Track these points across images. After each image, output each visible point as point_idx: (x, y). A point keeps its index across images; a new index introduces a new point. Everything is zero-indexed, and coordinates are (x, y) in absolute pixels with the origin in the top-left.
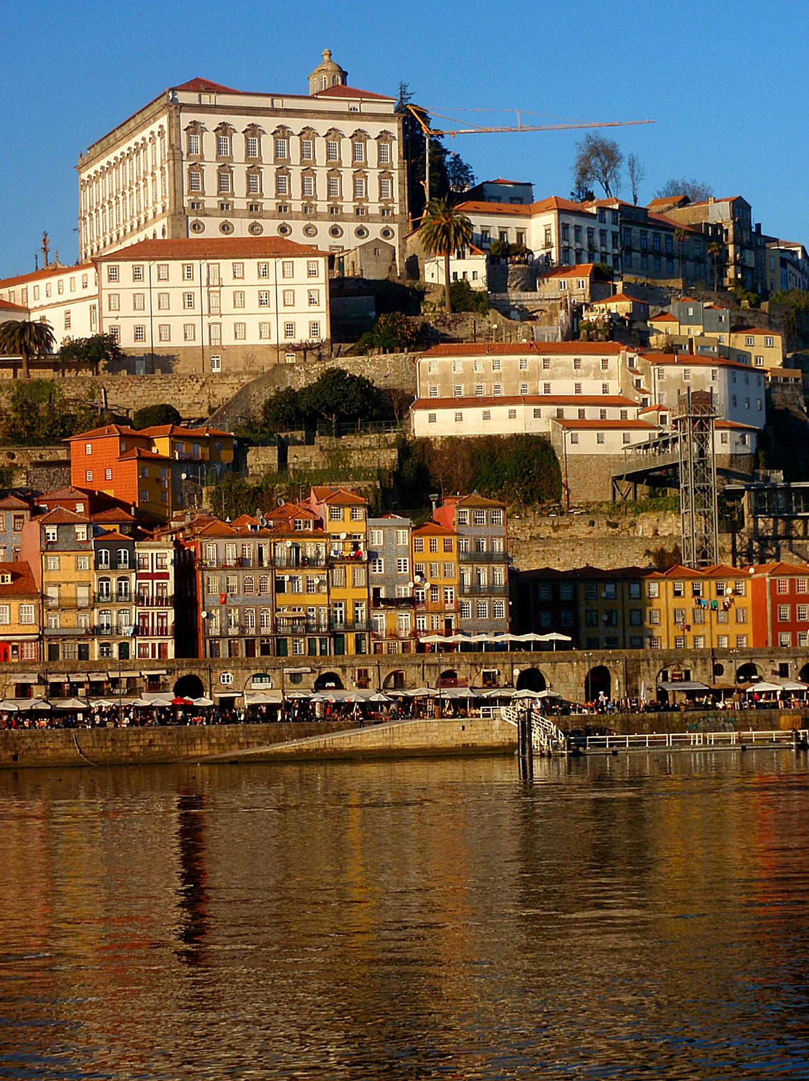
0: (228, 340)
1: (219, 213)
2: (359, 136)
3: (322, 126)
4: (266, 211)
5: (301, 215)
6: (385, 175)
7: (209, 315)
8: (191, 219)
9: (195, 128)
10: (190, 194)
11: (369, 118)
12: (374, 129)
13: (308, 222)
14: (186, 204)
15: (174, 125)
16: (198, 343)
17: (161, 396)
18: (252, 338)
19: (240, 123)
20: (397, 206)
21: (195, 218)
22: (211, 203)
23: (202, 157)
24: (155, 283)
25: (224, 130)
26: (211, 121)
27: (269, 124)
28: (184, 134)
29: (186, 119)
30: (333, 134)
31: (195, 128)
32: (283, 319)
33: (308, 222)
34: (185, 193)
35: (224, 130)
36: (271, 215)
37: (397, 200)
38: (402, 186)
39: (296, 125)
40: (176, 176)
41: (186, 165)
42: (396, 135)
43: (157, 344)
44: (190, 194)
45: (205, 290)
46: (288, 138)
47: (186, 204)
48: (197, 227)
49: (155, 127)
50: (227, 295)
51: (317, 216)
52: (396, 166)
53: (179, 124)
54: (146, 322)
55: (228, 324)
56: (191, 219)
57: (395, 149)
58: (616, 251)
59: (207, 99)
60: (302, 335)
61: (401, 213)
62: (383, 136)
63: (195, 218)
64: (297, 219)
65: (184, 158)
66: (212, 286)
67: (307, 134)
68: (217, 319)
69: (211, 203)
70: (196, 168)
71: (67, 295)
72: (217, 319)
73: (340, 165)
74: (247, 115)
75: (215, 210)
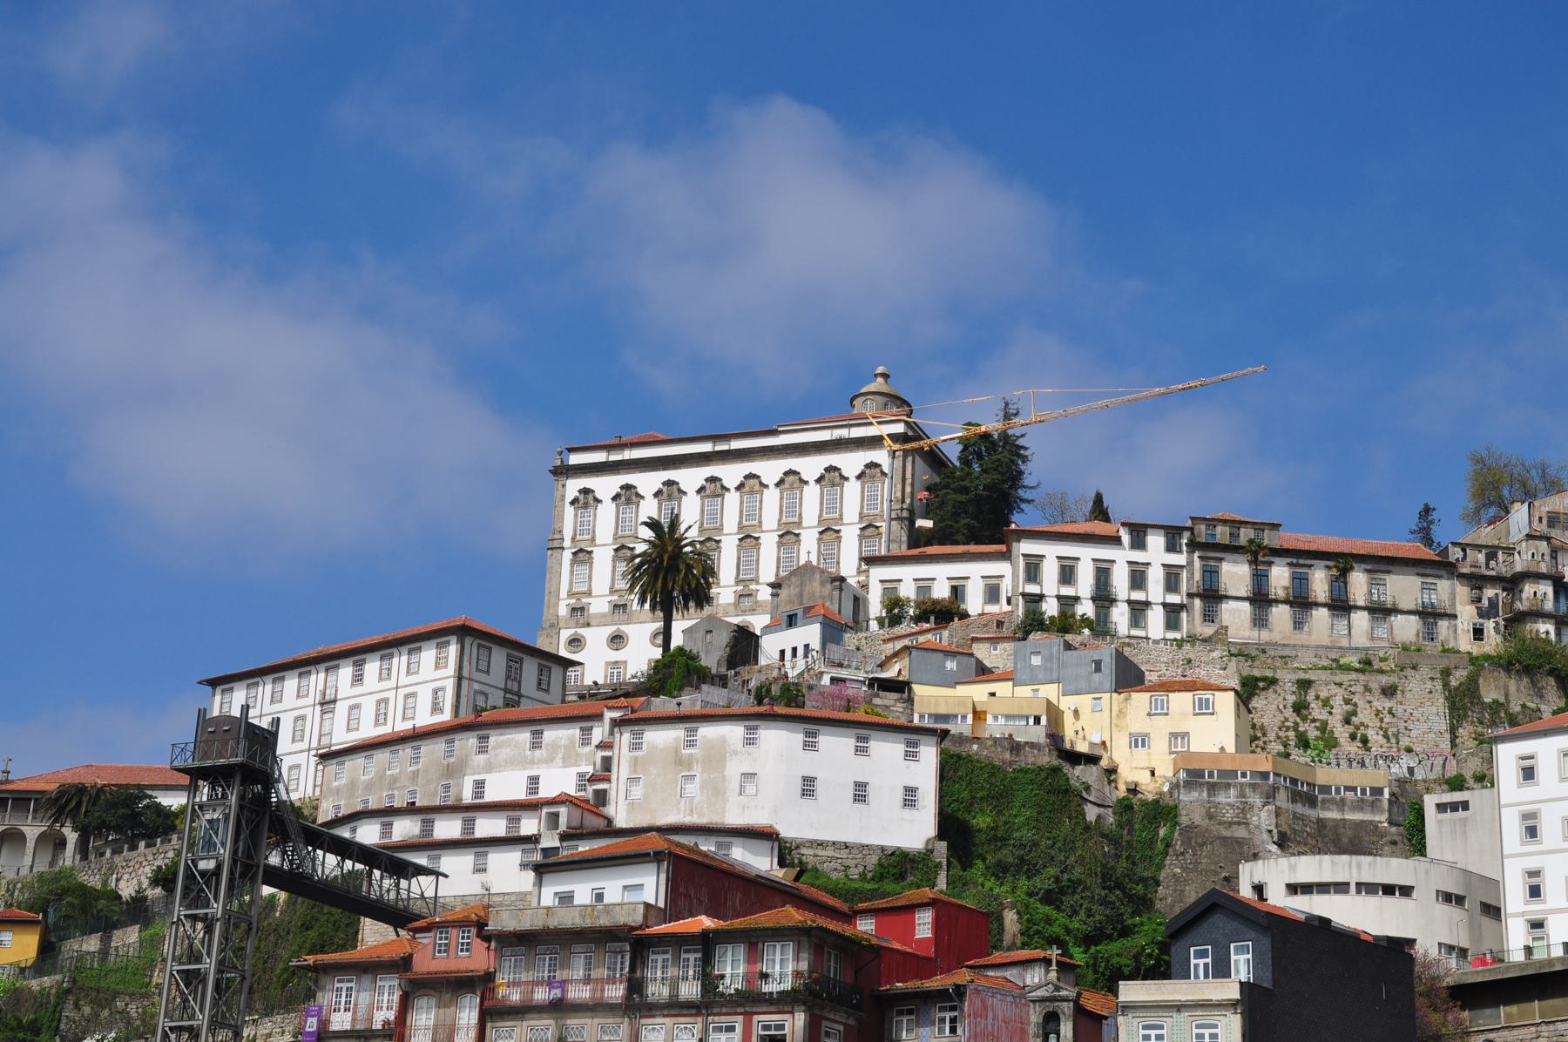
1: (609, 619)
8: (565, 634)
9: (587, 499)
10: (571, 595)
14: (563, 611)
21: (572, 631)
26: (605, 486)
29: (573, 486)
31: (587, 499)
39: (731, 473)
41: (567, 556)
46: (722, 496)
53: (563, 496)
58: (1174, 599)
63: (572, 631)
65: (567, 543)
73: (799, 524)
75: (603, 615)
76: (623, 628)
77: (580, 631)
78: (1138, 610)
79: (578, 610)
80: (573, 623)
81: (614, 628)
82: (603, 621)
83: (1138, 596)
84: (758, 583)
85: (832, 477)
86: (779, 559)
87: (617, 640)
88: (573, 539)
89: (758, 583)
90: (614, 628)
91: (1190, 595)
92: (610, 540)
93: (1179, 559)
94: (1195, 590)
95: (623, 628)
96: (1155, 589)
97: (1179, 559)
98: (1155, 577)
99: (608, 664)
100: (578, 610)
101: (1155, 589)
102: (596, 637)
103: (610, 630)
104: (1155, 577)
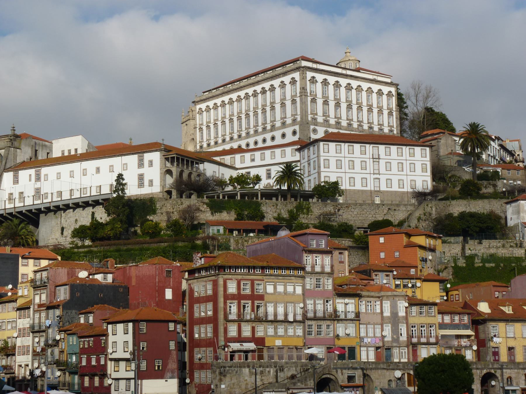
0: (383, 188)
2: (380, 93)
3: (365, 86)
6: (390, 114)
7: (374, 174)
8: (312, 127)
10: (311, 114)
11: (384, 84)
12: (386, 89)
14: (310, 119)
15: (303, 78)
16: (368, 188)
17: (366, 215)
18: (395, 188)
19: (332, 80)
20: (395, 130)
23: (316, 95)
24: (347, 155)
25: (325, 83)
26: (320, 77)
27: (344, 82)
28: (308, 83)
29: (309, 75)
30: (370, 91)
31: (313, 80)
32: (410, 178)
34: (309, 113)
35: (325, 83)
37: (395, 127)
39: (355, 84)
40: (303, 103)
41: (309, 99)
42: (394, 95)
43: (348, 188)
44: (311, 114)
45: (372, 160)
47: (310, 119)
48: (315, 131)
49: (287, 79)
50: (382, 163)
52: (394, 109)
54: (343, 175)
55: (383, 178)
56: (312, 127)
57: (394, 100)
59: (315, 66)
60: (419, 188)
62: (389, 94)
65: (309, 95)
66: (376, 159)
67: (359, 89)
68: (378, 176)
69: (320, 119)
70: (314, 101)
71: (268, 161)
72: (378, 176)
74: (335, 76)
81: (326, 129)
82: (321, 125)
95: (328, 129)
103: (325, 129)
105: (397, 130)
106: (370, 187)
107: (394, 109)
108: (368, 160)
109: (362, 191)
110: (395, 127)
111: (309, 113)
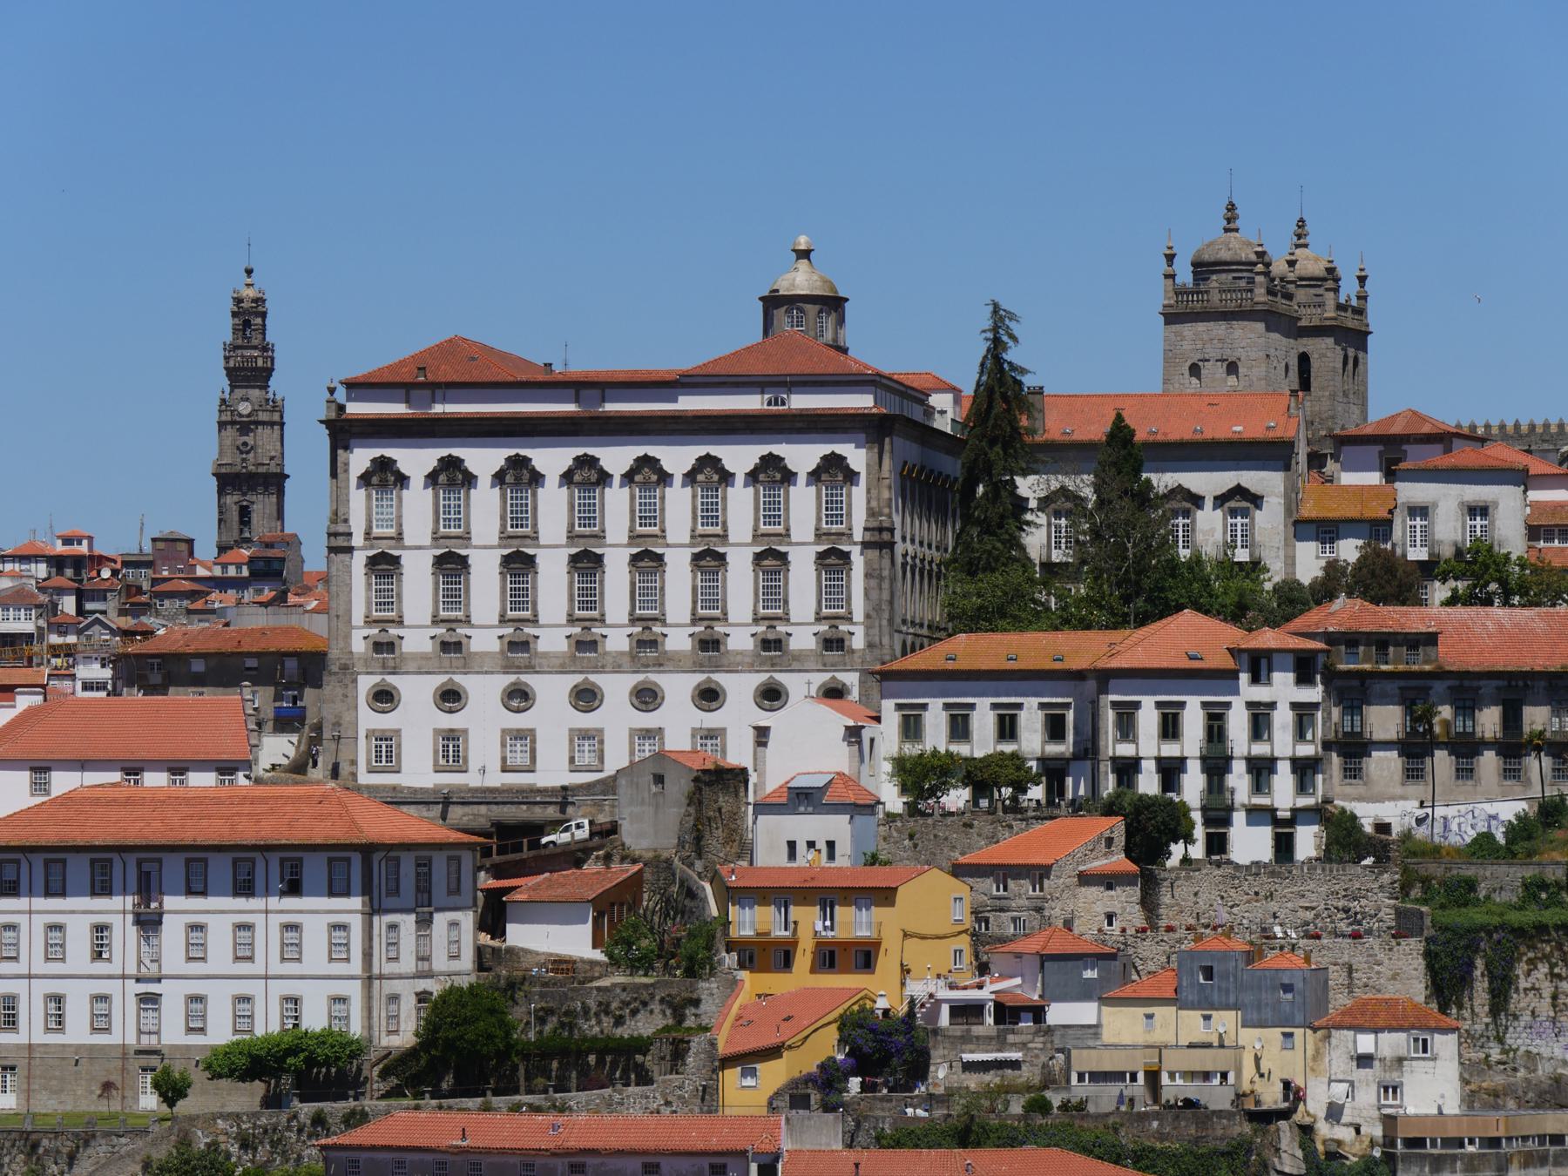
0: (173, 1032)
4: (546, 655)
5: (627, 659)
8: (366, 683)
10: (370, 622)
13: (640, 677)
14: (359, 645)
16: (114, 1039)
21: (377, 679)
22: (417, 640)
23: (399, 537)
32: (280, 988)
33: (640, 677)
36: (557, 662)
37: (859, 615)
38: (874, 583)
44: (370, 622)
48: (384, 697)
51: (664, 662)
55: (173, 995)
58: (1306, 750)
61: (870, 645)
63: (377, 679)
64: (618, 669)
65: (358, 540)
75: (424, 657)
76: (458, 678)
77: (391, 679)
78: (1261, 769)
79: (384, 647)
80: (377, 667)
81: (443, 678)
83: (1260, 749)
84: (664, 623)
85: (772, 473)
86: (694, 589)
87: (450, 697)
88: (368, 534)
89: (664, 623)
90: (443, 678)
91: (1327, 745)
92: (428, 541)
93: (1314, 694)
94: (1331, 736)
95: (458, 678)
96: (1283, 742)
97: (1314, 694)
98: (1283, 719)
99: (437, 732)
100: (384, 647)
101: (1283, 742)
102: (417, 691)
103: (439, 680)
104: (1283, 719)
105: (868, 628)
106: (124, 1033)
107: (858, 535)
108: (116, 921)
109: (92, 1048)
110: (859, 615)
111: (358, 616)
